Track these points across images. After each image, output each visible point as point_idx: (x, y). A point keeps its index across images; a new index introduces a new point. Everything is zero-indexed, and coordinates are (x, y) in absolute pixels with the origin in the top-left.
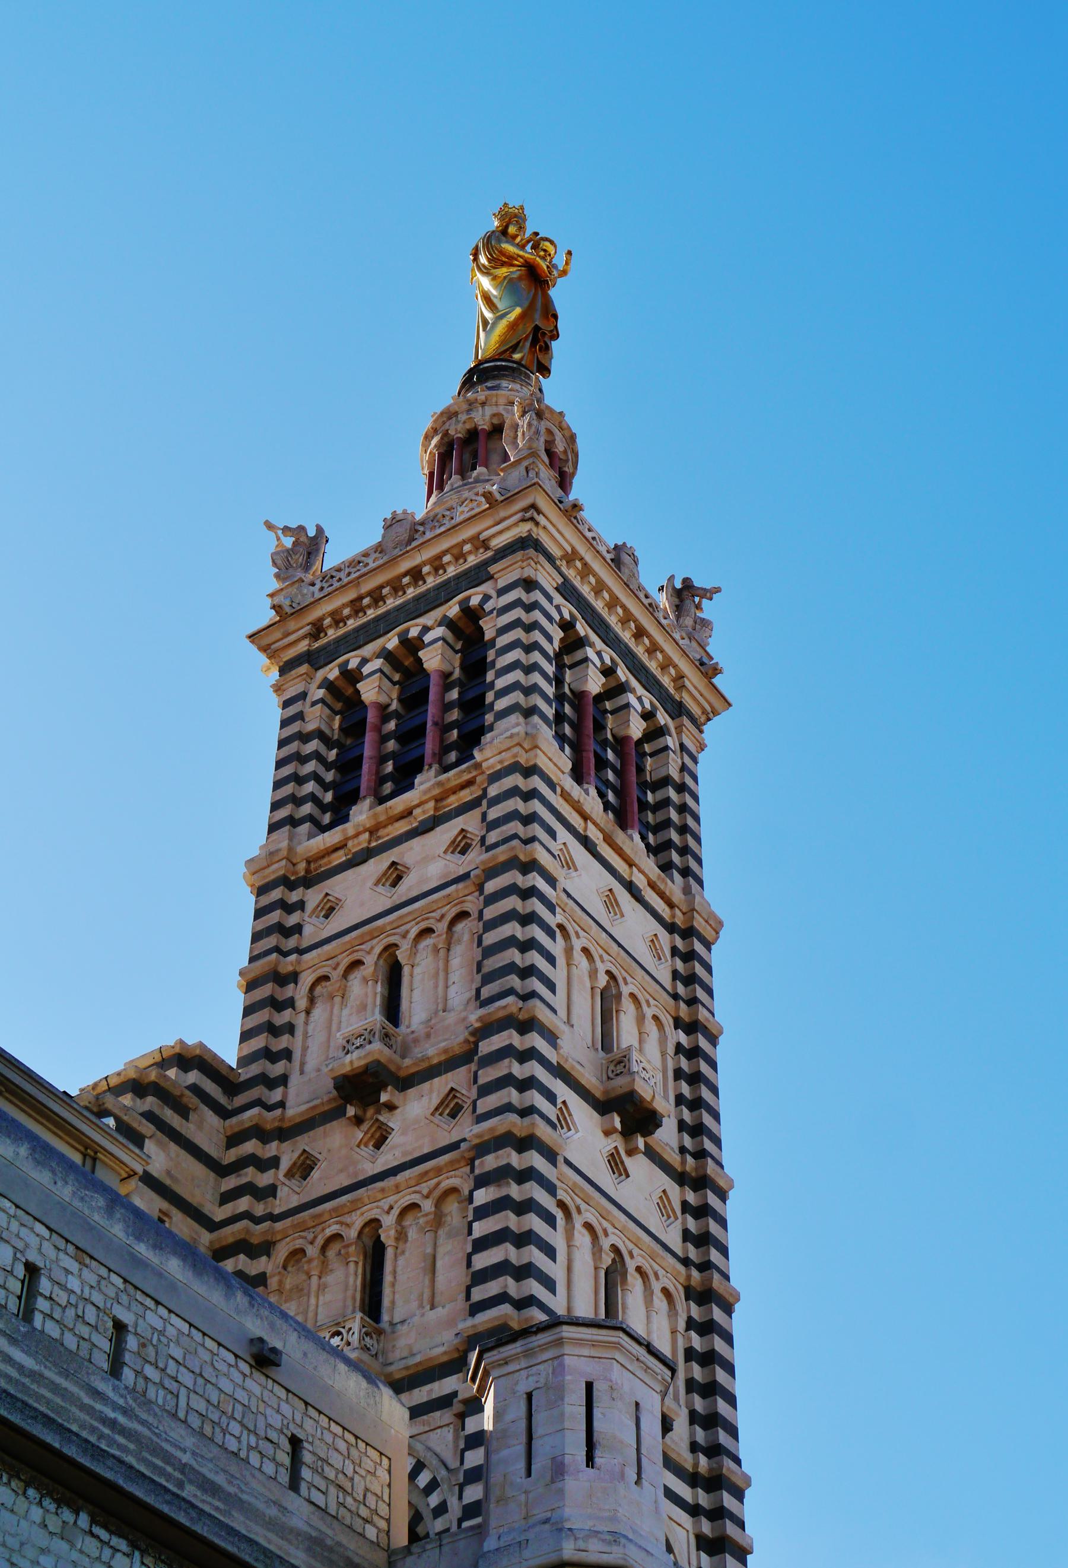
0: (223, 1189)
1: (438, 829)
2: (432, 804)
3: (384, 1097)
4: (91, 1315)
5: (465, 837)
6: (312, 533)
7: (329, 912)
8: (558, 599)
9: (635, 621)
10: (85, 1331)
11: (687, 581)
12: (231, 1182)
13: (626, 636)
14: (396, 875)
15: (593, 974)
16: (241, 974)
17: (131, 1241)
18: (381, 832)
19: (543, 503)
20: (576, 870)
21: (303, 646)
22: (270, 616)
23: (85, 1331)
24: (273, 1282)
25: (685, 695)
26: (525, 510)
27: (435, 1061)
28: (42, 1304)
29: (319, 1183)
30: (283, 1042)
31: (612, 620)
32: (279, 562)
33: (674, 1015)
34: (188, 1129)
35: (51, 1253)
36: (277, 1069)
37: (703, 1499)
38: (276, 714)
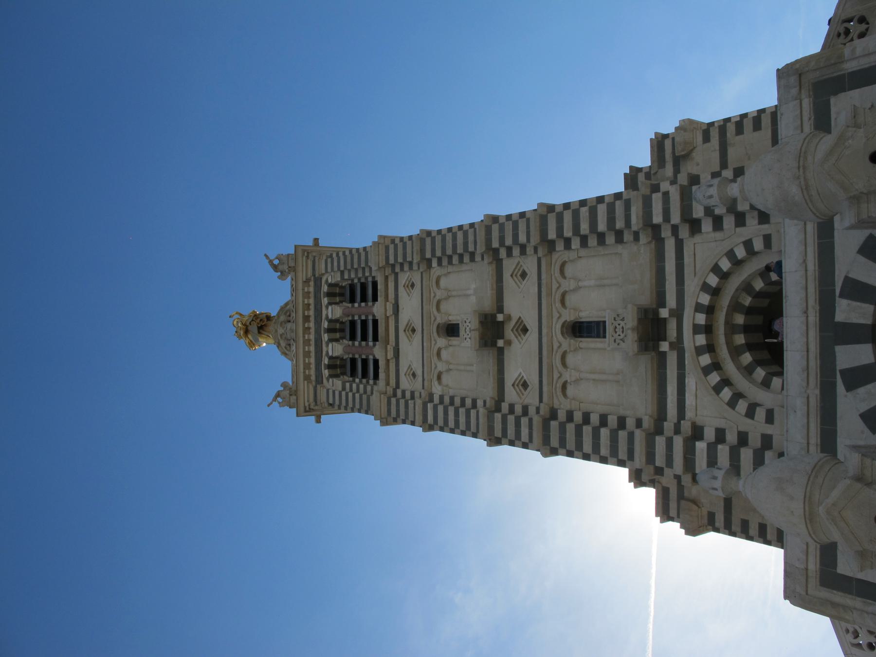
8: (325, 381)
9: (304, 325)
13: (312, 325)
15: (446, 347)
20: (410, 365)
31: (312, 337)
33: (429, 270)
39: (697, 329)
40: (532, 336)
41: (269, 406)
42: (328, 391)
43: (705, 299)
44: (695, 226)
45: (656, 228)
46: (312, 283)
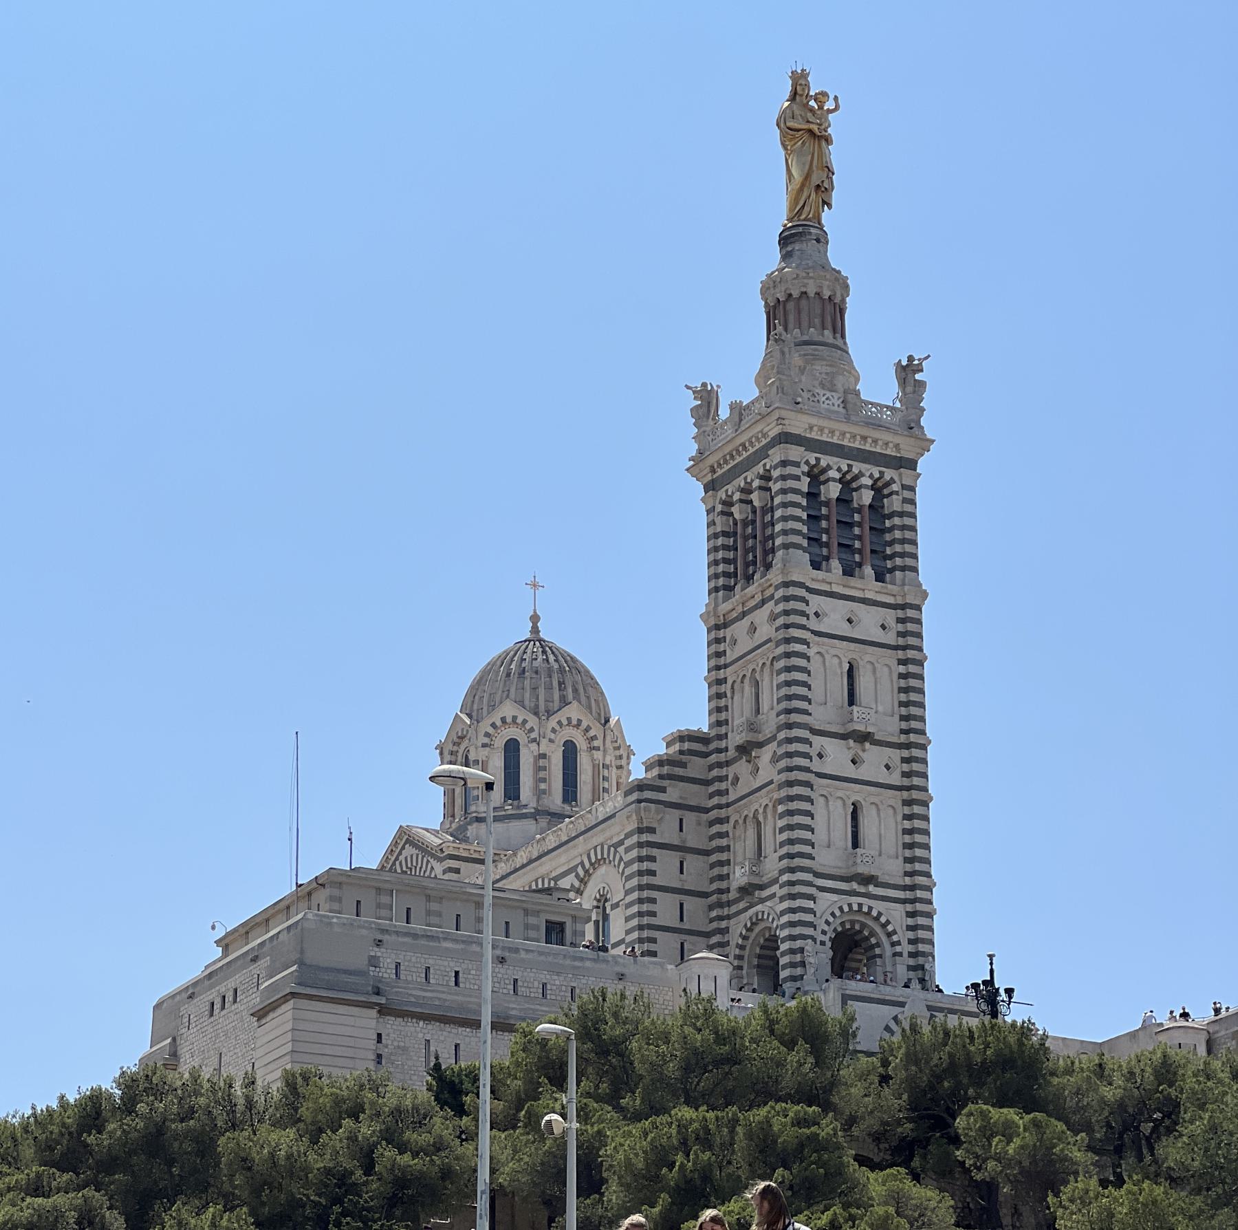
0: (710, 791)
2: (760, 594)
3: (753, 754)
4: (564, 988)
10: (563, 993)
11: (911, 358)
12: (711, 789)
14: (753, 629)
16: (705, 679)
17: (573, 963)
19: (784, 413)
22: (692, 463)
23: (563, 993)
24: (731, 834)
26: (777, 420)
27: (769, 736)
28: (548, 992)
29: (742, 789)
30: (723, 716)
31: (845, 443)
34: (690, 772)
35: (548, 977)
36: (723, 730)
37: (908, 895)
38: (704, 519)
39: (860, 905)
40: (850, 771)
42: (797, 464)
43: (874, 913)
44: (911, 915)
45: (912, 888)
46: (894, 454)
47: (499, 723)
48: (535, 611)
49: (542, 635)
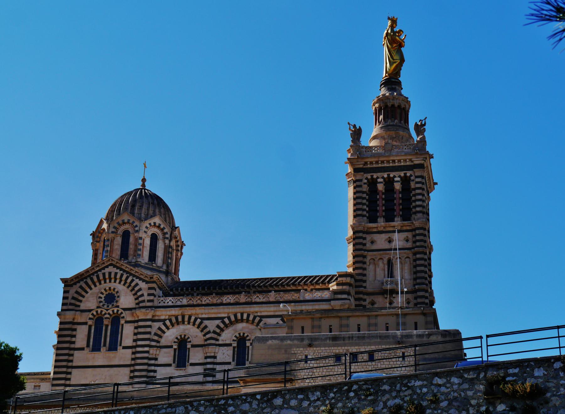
1: (401, 233)
5: (407, 238)
6: (358, 128)
7: (372, 242)
18: (386, 228)
21: (361, 166)
25: (430, 189)
26: (424, 158)
32: (352, 137)
41: (426, 118)
47: (152, 224)
48: (144, 177)
49: (146, 188)
